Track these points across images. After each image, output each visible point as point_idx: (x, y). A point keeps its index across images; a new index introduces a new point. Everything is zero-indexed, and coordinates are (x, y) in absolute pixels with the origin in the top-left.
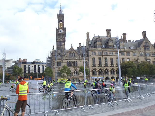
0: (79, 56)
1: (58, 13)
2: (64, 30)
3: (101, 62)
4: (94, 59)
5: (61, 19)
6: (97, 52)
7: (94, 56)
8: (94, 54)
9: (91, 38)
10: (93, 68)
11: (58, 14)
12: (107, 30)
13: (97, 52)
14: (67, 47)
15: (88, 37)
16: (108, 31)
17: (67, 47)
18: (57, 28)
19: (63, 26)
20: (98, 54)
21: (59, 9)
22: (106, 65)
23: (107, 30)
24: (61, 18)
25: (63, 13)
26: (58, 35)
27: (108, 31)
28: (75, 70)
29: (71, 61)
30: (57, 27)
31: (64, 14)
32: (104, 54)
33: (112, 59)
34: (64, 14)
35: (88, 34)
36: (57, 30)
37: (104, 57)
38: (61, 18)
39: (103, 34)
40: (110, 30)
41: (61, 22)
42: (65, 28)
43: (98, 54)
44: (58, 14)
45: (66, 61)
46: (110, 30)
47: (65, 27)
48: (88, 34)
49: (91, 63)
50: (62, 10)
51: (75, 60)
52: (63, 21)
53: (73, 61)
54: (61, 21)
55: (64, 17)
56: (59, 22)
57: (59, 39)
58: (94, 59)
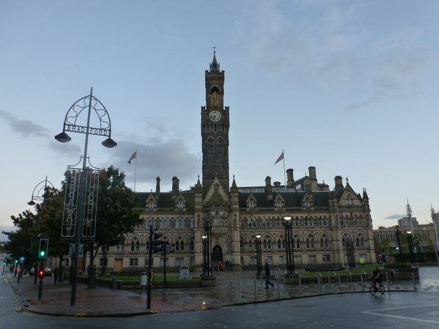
5: (217, 86)
11: (207, 71)
18: (203, 108)
21: (211, 61)
24: (215, 81)
30: (204, 104)
31: (223, 72)
34: (223, 72)
36: (205, 112)
38: (215, 81)
41: (215, 94)
44: (207, 71)
47: (226, 104)
50: (218, 61)
52: (220, 89)
54: (215, 89)
57: (209, 137)
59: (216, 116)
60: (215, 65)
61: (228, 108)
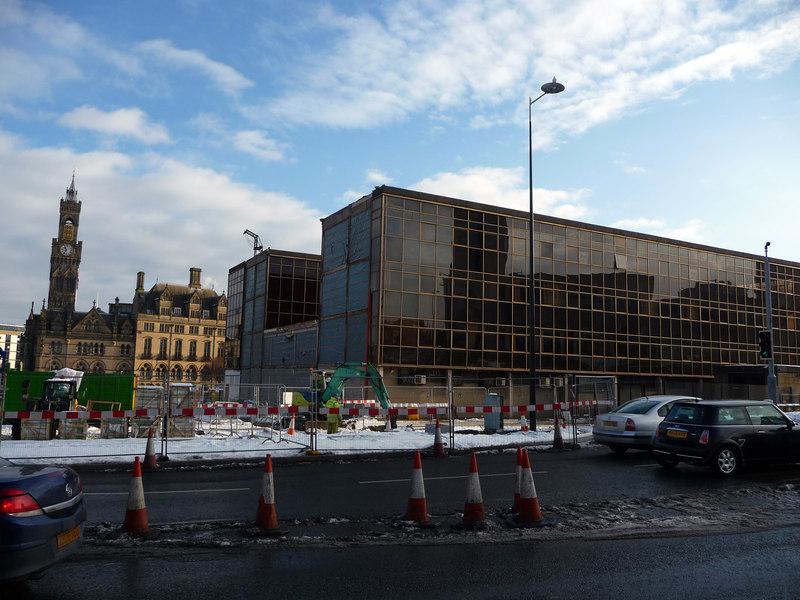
0: (109, 331)
1: (65, 197)
2: (78, 247)
3: (165, 348)
4: (149, 342)
6: (157, 325)
7: (150, 334)
8: (150, 328)
9: (147, 287)
10: (145, 361)
12: (192, 270)
13: (157, 325)
14: (82, 305)
15: (140, 285)
16: (195, 274)
17: (82, 305)
19: (75, 235)
20: (161, 331)
22: (178, 357)
23: (192, 270)
25: (78, 198)
26: (57, 260)
27: (195, 274)
28: (98, 365)
29: (88, 342)
30: (56, 236)
32: (177, 331)
33: (193, 344)
35: (141, 275)
36: (56, 244)
37: (175, 336)
38: (70, 210)
39: (183, 282)
40: (199, 271)
42: (80, 243)
43: (161, 331)
45: (77, 341)
46: (199, 271)
47: (79, 239)
48: (141, 275)
49: (139, 350)
50: (76, 188)
51: (99, 339)
53: (94, 342)
55: (79, 211)
56: (62, 223)
58: (149, 342)
59: (68, 250)
60: (71, 192)
61: (80, 243)
